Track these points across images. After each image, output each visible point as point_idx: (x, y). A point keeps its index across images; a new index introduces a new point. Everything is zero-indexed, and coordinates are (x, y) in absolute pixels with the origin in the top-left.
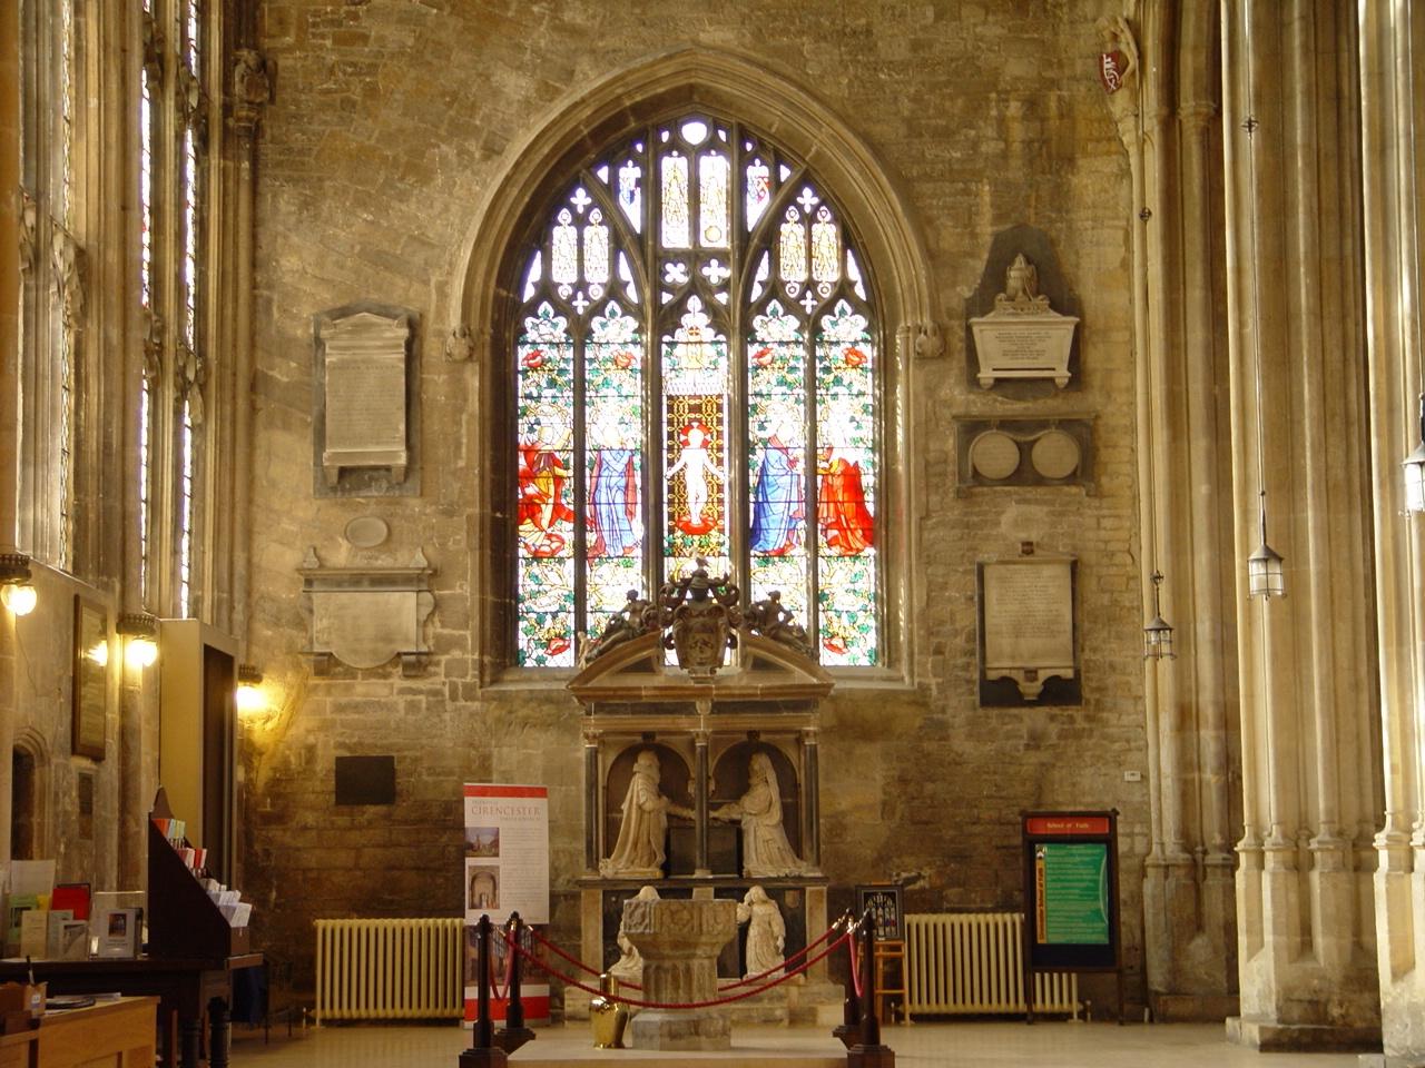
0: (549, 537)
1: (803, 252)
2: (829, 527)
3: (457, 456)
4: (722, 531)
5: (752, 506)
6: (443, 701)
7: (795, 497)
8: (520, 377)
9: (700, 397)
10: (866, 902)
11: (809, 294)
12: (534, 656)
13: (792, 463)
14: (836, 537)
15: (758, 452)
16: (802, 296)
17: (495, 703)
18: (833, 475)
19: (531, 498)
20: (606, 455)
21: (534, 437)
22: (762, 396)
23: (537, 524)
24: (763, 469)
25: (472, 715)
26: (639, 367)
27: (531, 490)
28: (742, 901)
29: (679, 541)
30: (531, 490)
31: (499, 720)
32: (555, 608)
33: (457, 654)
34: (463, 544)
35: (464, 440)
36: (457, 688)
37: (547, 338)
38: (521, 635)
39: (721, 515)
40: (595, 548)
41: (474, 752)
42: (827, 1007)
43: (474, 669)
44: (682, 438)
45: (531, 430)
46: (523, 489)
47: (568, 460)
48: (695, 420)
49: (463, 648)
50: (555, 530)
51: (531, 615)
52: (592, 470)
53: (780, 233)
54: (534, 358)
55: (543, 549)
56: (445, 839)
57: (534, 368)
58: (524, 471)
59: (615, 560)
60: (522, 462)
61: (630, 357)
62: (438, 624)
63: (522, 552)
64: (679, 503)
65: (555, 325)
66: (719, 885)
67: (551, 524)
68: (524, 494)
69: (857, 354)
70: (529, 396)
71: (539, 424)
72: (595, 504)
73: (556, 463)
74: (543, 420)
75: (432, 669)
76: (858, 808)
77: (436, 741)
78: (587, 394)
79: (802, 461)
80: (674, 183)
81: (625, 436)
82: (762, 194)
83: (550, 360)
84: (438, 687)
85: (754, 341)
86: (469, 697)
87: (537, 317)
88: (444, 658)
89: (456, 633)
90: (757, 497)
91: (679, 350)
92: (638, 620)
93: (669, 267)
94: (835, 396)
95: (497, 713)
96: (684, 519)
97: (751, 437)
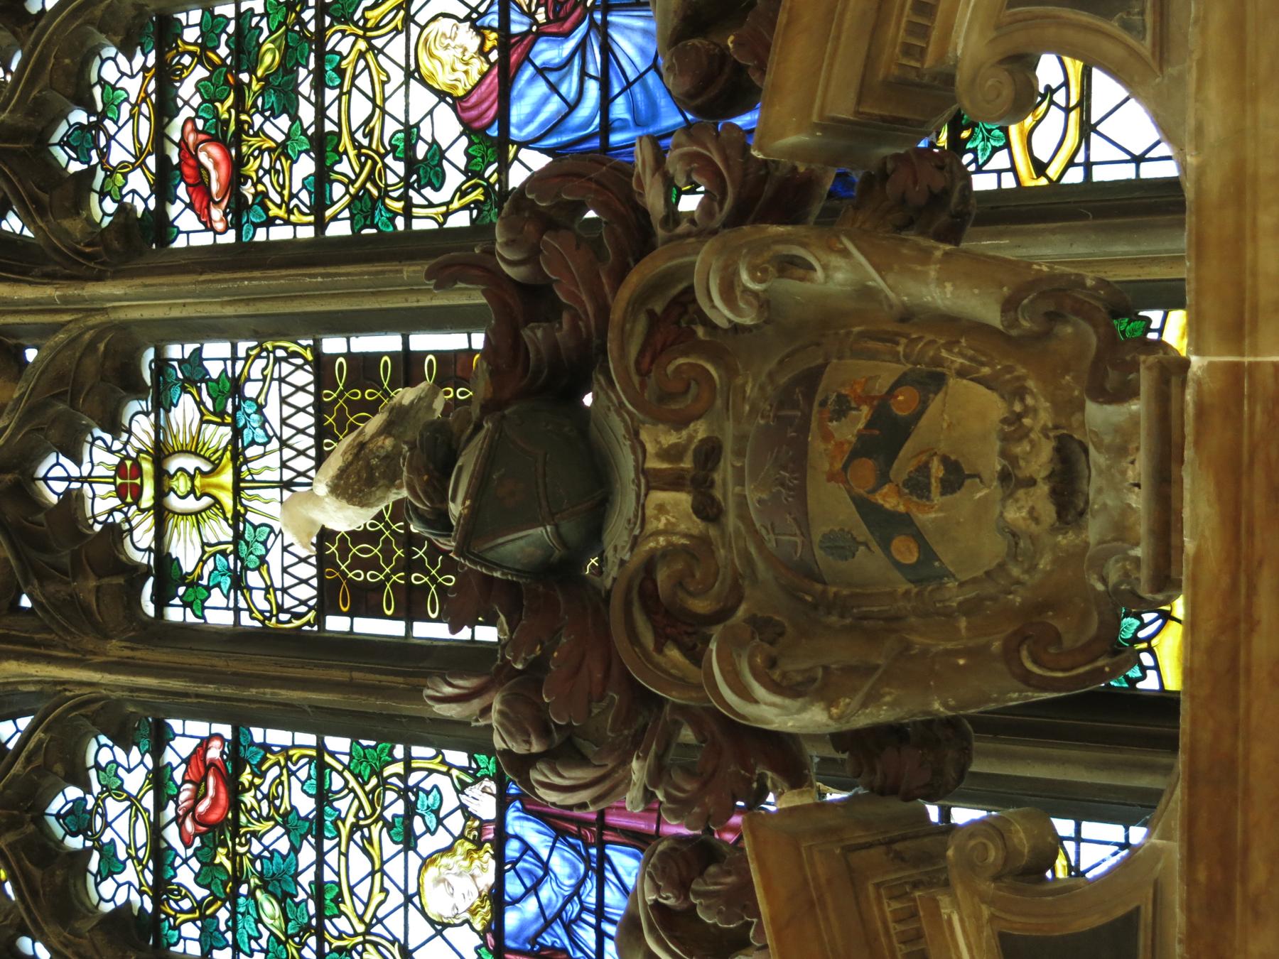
22: (322, 179)
85: (160, 226)
91: (185, 550)
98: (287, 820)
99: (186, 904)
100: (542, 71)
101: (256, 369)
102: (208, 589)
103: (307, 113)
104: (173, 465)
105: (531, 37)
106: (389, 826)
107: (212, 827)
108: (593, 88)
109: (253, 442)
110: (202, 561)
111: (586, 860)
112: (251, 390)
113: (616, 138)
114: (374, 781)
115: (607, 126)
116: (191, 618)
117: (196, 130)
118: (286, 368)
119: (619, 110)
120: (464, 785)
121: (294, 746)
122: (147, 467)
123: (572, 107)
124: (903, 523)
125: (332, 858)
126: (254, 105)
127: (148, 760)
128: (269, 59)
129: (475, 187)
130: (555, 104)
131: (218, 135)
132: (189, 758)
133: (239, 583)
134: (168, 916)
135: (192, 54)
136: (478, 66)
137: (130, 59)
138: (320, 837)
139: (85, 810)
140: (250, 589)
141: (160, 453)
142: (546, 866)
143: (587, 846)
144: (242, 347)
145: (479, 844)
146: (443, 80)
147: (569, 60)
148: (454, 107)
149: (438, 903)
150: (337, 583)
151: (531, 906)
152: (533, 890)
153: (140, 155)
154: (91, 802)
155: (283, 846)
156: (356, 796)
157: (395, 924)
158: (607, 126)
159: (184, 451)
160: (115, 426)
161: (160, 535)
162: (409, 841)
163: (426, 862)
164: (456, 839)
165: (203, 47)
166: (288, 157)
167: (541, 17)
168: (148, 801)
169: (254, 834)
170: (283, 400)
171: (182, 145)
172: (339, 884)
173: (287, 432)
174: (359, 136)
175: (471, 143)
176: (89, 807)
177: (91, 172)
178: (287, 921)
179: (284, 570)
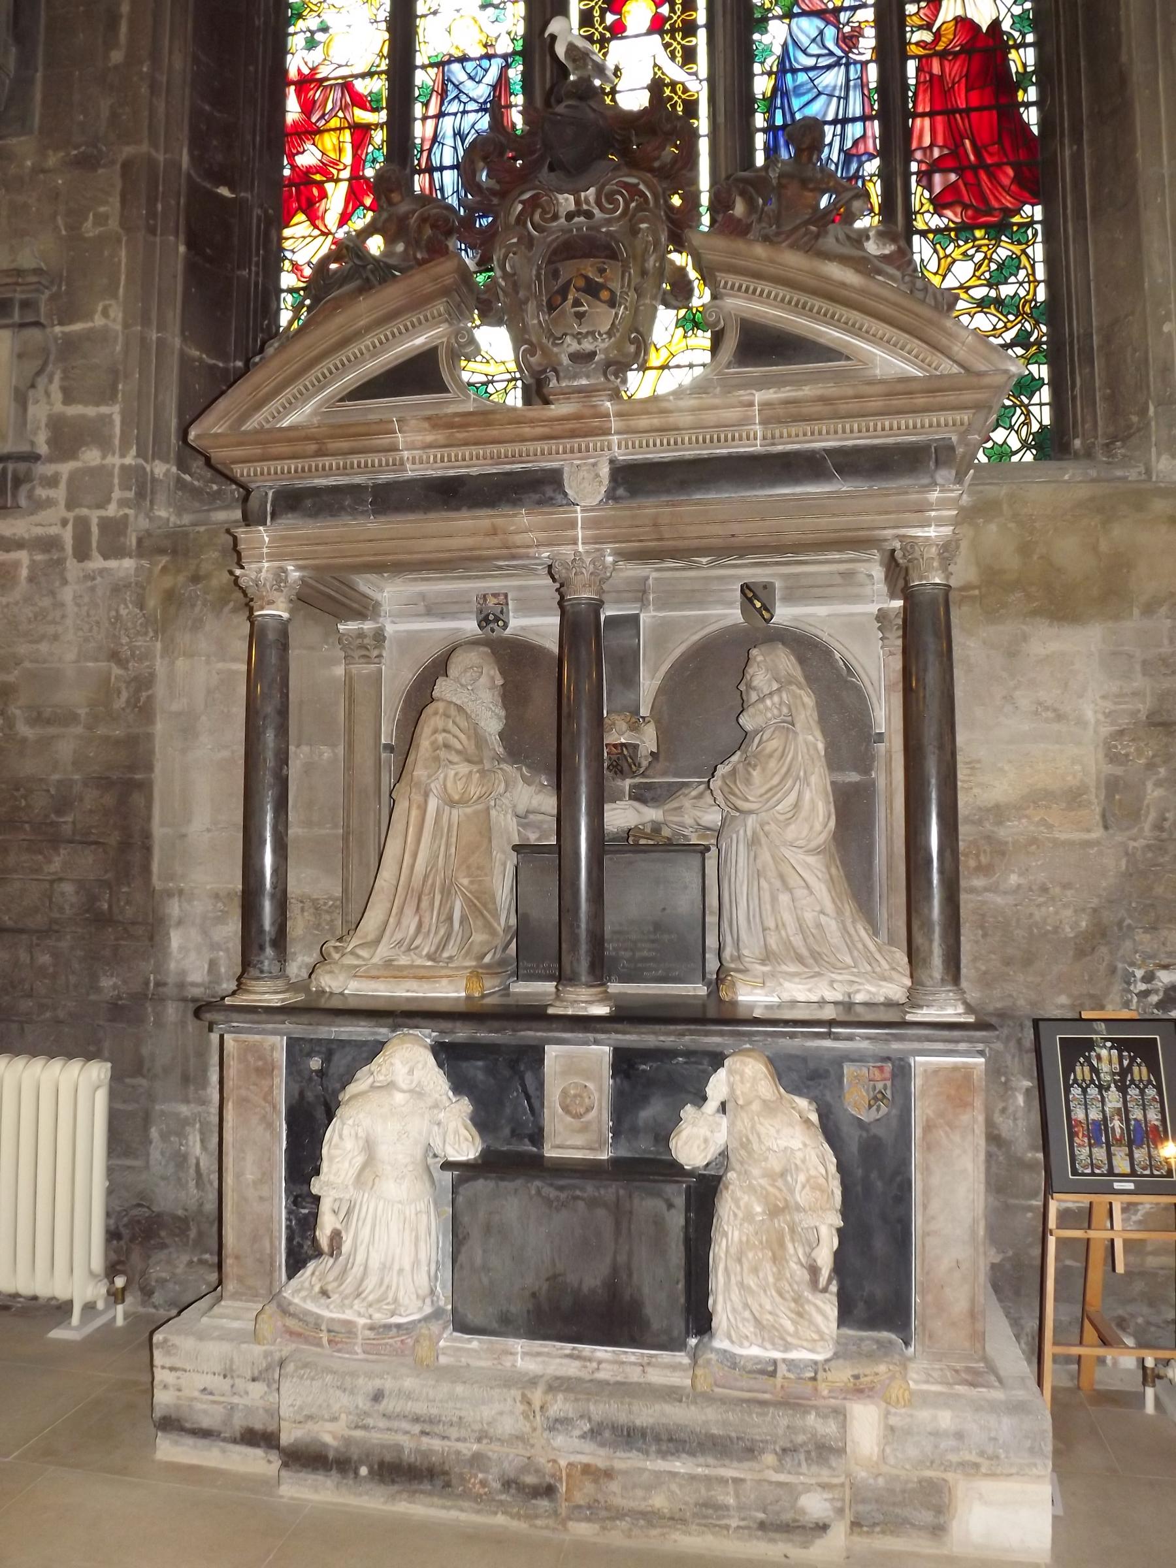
2: (937, 166)
3: (110, 43)
5: (760, 140)
6: (60, 562)
7: (855, 107)
10: (1069, 1069)
13: (849, 41)
14: (949, 189)
15: (774, 25)
17: (164, 560)
18: (943, 55)
19: (310, 170)
20: (457, 71)
21: (315, 56)
24: (785, 67)
25: (116, 590)
27: (308, 158)
28: (701, 1098)
30: (308, 158)
31: (170, 597)
33: (91, 457)
34: (114, 224)
35: (125, 8)
36: (88, 531)
41: (116, 671)
42: (987, 1486)
43: (125, 487)
44: (610, 18)
45: (311, 44)
46: (291, 157)
49: (104, 444)
52: (426, 105)
56: (56, 865)
58: (295, 124)
62: (57, 396)
66: (634, 1038)
68: (294, 167)
71: (325, 29)
72: (430, 170)
73: (359, 101)
74: (329, 17)
75: (42, 493)
76: (1038, 798)
77: (44, 647)
79: (870, 32)
81: (493, 30)
84: (54, 530)
86: (113, 551)
88: (65, 469)
89: (91, 411)
90: (770, 119)
92: (400, 247)
95: (168, 582)
100: (821, 33)
105: (837, 25)
108: (810, 62)
111: (485, 102)
113: (789, 76)
115: (794, 71)
119: (802, 77)
120: (509, 33)
123: (804, 52)
124: (565, 299)
130: (804, 41)
142: (479, 82)
145: (485, 46)
147: (825, 47)
152: (471, 78)
158: (794, 71)
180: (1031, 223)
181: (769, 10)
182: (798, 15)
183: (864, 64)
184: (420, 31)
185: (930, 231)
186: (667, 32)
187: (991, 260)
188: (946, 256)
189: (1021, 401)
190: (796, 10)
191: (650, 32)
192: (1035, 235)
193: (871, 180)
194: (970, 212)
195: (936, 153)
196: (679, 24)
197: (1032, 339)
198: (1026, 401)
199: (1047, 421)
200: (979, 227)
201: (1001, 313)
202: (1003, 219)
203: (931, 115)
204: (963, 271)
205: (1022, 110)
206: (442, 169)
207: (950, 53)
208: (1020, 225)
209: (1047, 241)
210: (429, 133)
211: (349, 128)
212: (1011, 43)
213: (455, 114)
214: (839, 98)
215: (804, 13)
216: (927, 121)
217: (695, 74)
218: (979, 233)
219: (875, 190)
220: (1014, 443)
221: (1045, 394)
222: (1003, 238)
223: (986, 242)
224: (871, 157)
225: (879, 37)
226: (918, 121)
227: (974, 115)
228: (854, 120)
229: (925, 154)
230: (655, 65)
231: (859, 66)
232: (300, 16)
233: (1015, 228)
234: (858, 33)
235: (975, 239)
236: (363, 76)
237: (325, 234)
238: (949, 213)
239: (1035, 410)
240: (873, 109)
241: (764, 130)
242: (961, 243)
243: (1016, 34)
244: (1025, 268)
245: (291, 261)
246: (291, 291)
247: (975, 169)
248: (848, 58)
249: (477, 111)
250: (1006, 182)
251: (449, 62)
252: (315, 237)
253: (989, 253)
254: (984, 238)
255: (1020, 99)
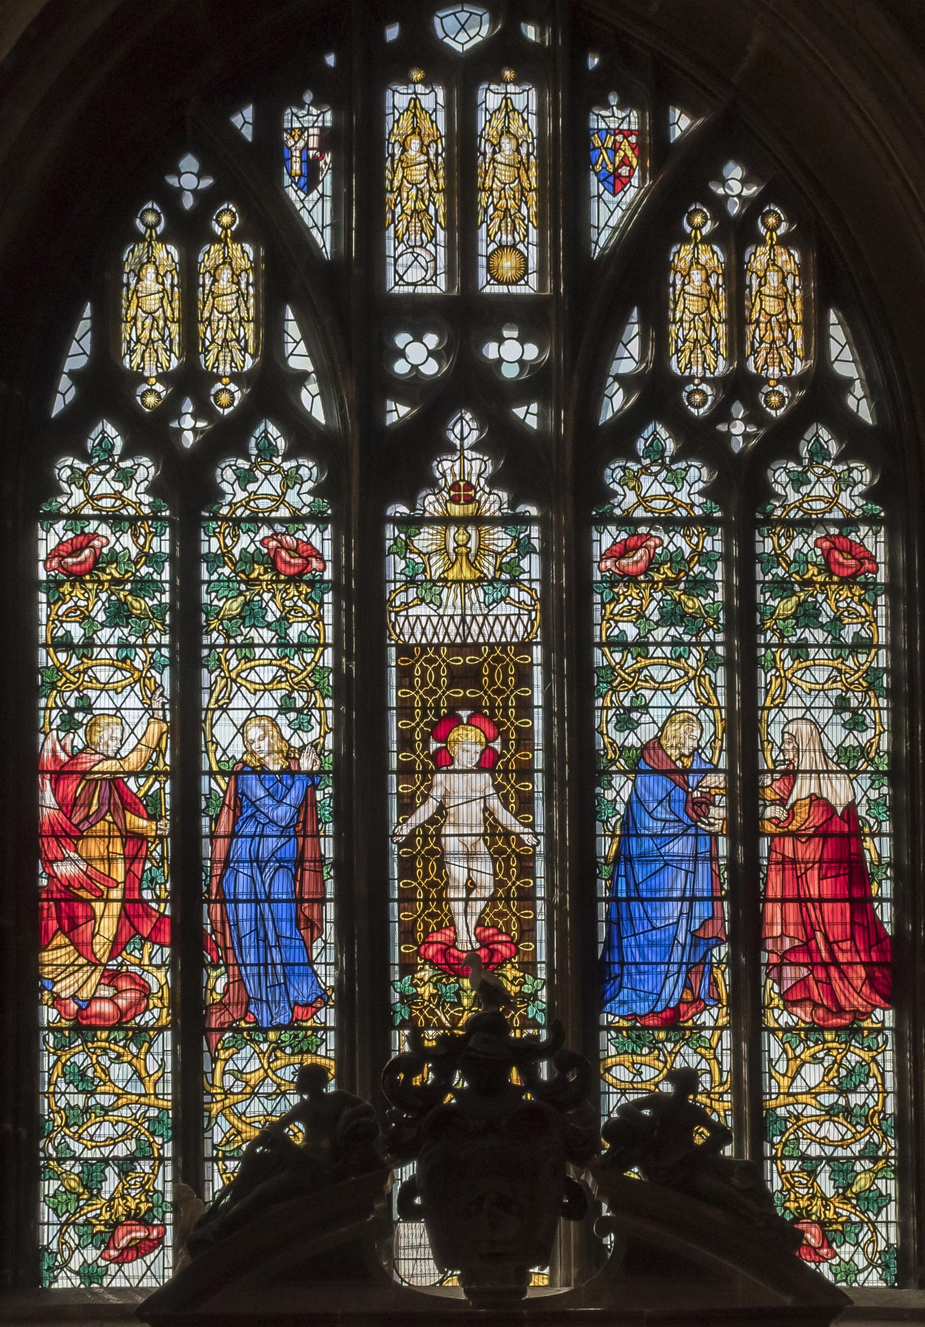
0: (112, 977)
1: (720, 310)
2: (785, 959)
4: (529, 967)
5: (603, 907)
8: (43, 597)
9: (476, 648)
11: (739, 411)
12: (75, 1264)
15: (617, 781)
16: (722, 413)
18: (795, 835)
23: (82, 947)
24: (628, 821)
26: (328, 575)
29: (427, 991)
32: (121, 1151)
37: (106, 503)
38: (46, 1213)
39: (527, 931)
40: (223, 1005)
44: (434, 746)
45: (69, 725)
47: (156, 799)
48: (465, 703)
50: (132, 956)
51: (67, 1166)
52: (216, 819)
53: (667, 267)
54: (76, 551)
55: (97, 1007)
57: (76, 578)
59: (272, 1035)
60: (48, 798)
61: (309, 553)
63: (49, 1015)
64: (426, 900)
65: (126, 477)
67: (117, 946)
69: (853, 550)
70: (65, 644)
71: (88, 708)
73: (129, 803)
78: (206, 641)
80: (415, 143)
82: (624, 171)
83: (114, 558)
85: (606, 520)
87: (86, 457)
90: (613, 888)
91: (425, 539)
93: (402, 339)
94: (800, 649)
96: (438, 937)
97: (600, 742)
98: (284, 620)
99: (229, 542)
101: (525, 596)
102: (405, 558)
103: (659, 634)
104: (471, 530)
106: (289, 696)
107: (274, 562)
109: (485, 594)
110: (420, 553)
111: (287, 827)
112: (514, 592)
114: (311, 684)
115: (639, 836)
116: (389, 543)
117: (656, 547)
118: (525, 618)
119: (648, 844)
120: (316, 747)
121: (324, 625)
122: (471, 508)
125: (268, 654)
126: (667, 593)
127: (306, 511)
128: (691, 604)
129: (615, 752)
131: (652, 564)
132: (310, 544)
133: (411, 582)
134: (220, 527)
135: (697, 545)
136: (674, 753)
137: (700, 493)
138: (278, 645)
139: (272, 456)
140: (406, 591)
141: (478, 520)
142: (280, 802)
143: (294, 826)
144: (536, 586)
145: (287, 758)
146: (670, 730)
148: (656, 737)
149: (254, 732)
150: (412, 656)
151: (261, 793)
153: (643, 501)
154: (277, 461)
155: (270, 618)
156: (302, 671)
157: (238, 702)
158: (639, 836)
159: (480, 537)
160: (493, 482)
161: (433, 521)
162: (283, 709)
163: (273, 721)
164: (287, 741)
165: (700, 554)
166: (637, 619)
167: (696, 794)
168: (284, 512)
169: (274, 596)
170: (508, 616)
171: (649, 536)
172: (254, 660)
173: (491, 619)
174: (645, 672)
175: (637, 749)
176: (275, 459)
177: (637, 460)
178: (230, 620)
179: (418, 617)
180: (880, 1031)
181: (613, 762)
182: (646, 772)
183: (714, 836)
184: (208, 728)
185: (780, 1029)
186: (499, 771)
187: (840, 1065)
188: (796, 1057)
189: (869, 1218)
190: (642, 765)
191: (480, 768)
192: (885, 1042)
193: (718, 968)
194: (821, 1012)
195: (787, 945)
196: (513, 766)
197: (880, 1153)
198: (873, 1218)
199: (893, 1240)
200: (830, 1029)
201: (850, 1123)
202: (852, 1023)
203: (783, 901)
204: (813, 1075)
205: (876, 904)
206: (236, 901)
207: (803, 836)
208: (871, 1030)
209: (899, 1051)
210: (220, 853)
211: (121, 836)
212: (867, 830)
213: (253, 837)
214: (687, 872)
215: (654, 772)
216: (778, 907)
217: (532, 825)
218: (829, 1036)
219: (723, 978)
220: (861, 1261)
221: (892, 1212)
222: (853, 1042)
223: (835, 1045)
224: (719, 942)
225: (731, 808)
226: (769, 906)
227: (827, 907)
228: (702, 899)
229: (775, 944)
230: (486, 809)
231: (708, 838)
232: (53, 686)
233: (866, 1032)
234: (708, 801)
235: (825, 1042)
236: (136, 774)
237: (94, 963)
238: (799, 1011)
239: (882, 1229)
240: (722, 889)
241: (607, 900)
242: (812, 1044)
243: (872, 821)
244: (874, 1076)
245: (51, 991)
246: (51, 1029)
247: (825, 966)
248: (697, 827)
249: (279, 837)
250: (858, 983)
251: (242, 772)
252: (81, 966)
253: (839, 1057)
254: (833, 1041)
255: (874, 892)
